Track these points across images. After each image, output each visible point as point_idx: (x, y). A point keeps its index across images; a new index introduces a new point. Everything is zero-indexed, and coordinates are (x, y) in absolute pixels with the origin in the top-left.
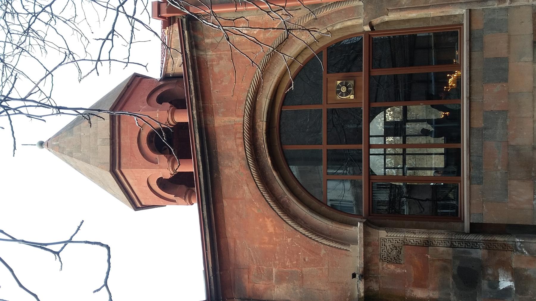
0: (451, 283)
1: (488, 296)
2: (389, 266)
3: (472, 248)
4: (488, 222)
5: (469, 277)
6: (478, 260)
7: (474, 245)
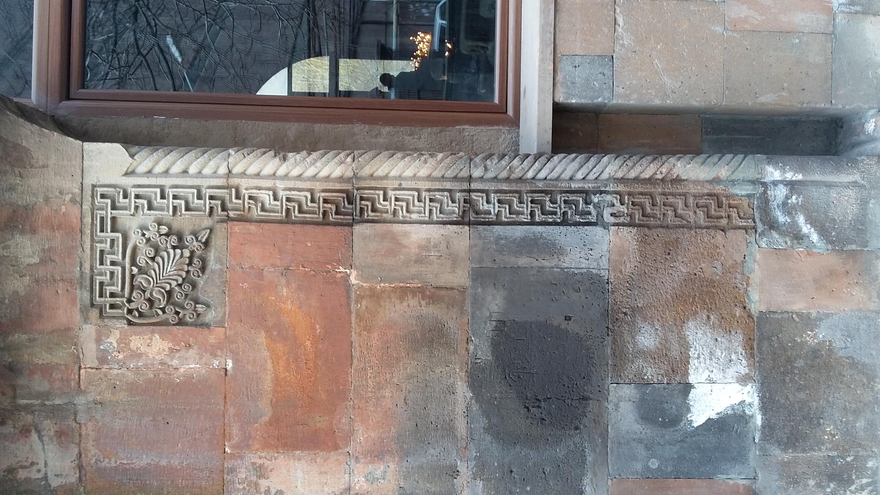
0: (460, 409)
1: (639, 466)
2: (137, 342)
3: (564, 222)
4: (633, 101)
5: (547, 369)
6: (594, 283)
7: (574, 209)
